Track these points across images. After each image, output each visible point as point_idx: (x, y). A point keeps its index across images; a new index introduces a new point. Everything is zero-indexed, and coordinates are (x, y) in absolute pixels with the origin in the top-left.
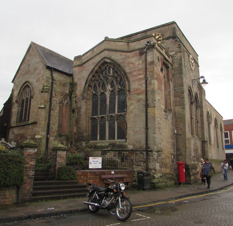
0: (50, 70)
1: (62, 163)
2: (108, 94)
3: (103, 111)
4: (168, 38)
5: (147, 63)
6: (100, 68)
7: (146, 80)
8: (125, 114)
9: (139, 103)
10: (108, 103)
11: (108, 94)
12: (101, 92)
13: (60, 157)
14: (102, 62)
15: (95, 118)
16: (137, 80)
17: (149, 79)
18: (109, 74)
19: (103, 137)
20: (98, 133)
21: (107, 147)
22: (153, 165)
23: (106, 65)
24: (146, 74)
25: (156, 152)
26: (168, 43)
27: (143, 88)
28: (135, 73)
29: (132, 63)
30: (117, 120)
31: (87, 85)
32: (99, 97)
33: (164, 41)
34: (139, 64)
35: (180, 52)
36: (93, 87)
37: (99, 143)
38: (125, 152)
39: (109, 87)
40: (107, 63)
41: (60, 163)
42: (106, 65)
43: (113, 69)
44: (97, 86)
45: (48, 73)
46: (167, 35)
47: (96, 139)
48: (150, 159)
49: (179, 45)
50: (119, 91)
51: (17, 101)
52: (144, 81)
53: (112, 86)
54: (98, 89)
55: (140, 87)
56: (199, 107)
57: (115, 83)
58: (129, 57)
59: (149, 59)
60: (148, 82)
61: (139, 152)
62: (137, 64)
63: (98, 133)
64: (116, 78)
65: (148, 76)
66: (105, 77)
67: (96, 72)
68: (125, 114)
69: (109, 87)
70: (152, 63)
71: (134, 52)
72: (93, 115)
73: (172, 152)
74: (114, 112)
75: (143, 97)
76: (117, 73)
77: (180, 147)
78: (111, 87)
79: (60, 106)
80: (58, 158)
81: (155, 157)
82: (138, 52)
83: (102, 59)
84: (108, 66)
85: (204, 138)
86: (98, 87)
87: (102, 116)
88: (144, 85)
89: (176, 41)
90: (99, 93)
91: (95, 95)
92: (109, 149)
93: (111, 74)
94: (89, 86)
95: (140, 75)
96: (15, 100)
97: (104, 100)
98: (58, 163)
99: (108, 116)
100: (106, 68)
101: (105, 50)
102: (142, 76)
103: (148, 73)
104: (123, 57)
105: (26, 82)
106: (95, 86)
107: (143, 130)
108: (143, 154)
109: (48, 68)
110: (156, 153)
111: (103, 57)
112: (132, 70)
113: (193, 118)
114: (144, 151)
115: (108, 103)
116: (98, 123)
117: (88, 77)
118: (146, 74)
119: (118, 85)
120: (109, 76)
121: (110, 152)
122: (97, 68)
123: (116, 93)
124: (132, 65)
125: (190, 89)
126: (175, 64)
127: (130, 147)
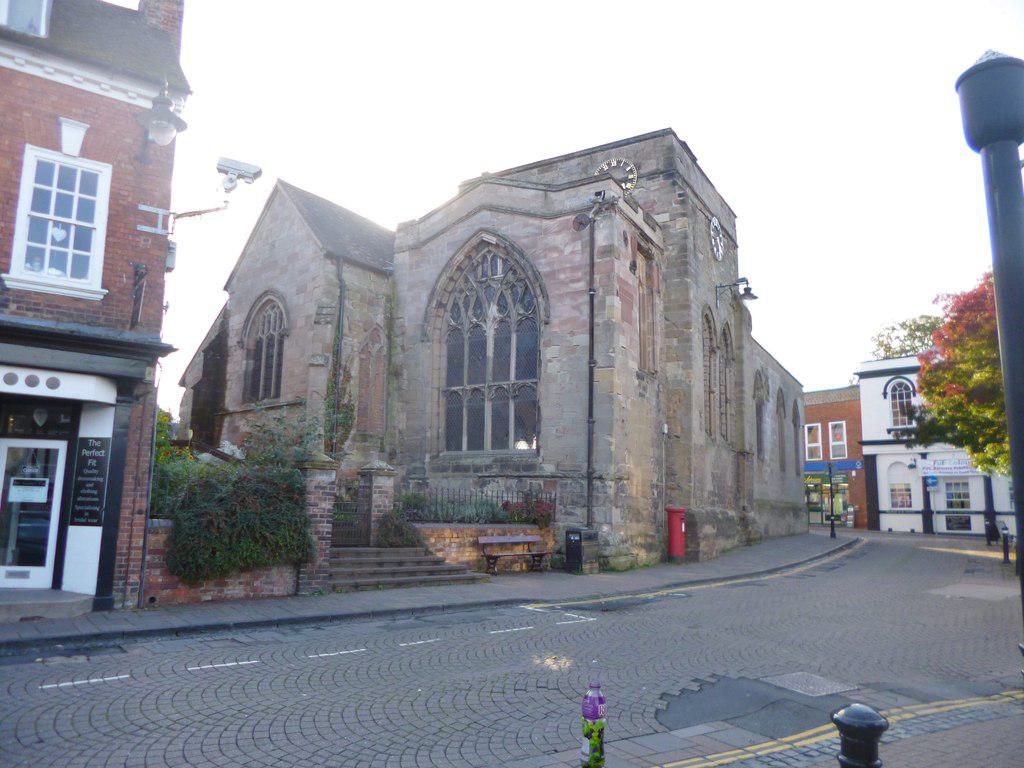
0: (334, 261)
1: (385, 507)
2: (490, 330)
3: (478, 375)
4: (651, 176)
5: (596, 251)
6: (468, 257)
7: (592, 297)
8: (536, 383)
9: (572, 356)
10: (490, 352)
11: (490, 330)
12: (471, 323)
13: (380, 492)
14: (475, 241)
15: (456, 392)
16: (568, 294)
17: (600, 292)
18: (493, 275)
19: (476, 443)
20: (465, 431)
21: (488, 467)
22: (605, 513)
23: (486, 249)
24: (591, 281)
25: (612, 480)
26: (652, 189)
27: (585, 316)
28: (562, 276)
29: (555, 249)
30: (514, 397)
31: (435, 302)
32: (466, 336)
33: (643, 182)
34: (573, 252)
35: (684, 215)
36: (449, 307)
37: (467, 457)
38: (534, 482)
39: (493, 311)
40: (489, 244)
41: (380, 506)
42: (486, 249)
43: (505, 261)
44: (461, 305)
45: (331, 268)
46: (651, 165)
47: (459, 448)
48: (597, 498)
49: (680, 195)
50: (520, 322)
51: (240, 343)
52: (586, 298)
53: (502, 307)
54: (463, 315)
55: (576, 314)
56: (733, 360)
57: (510, 300)
58: (546, 231)
59: (601, 240)
60: (596, 301)
61: (569, 481)
62: (568, 250)
63: (465, 431)
64: (513, 286)
65: (596, 285)
66: (481, 282)
67: (459, 269)
68: (536, 383)
69: (493, 311)
70: (609, 251)
71: (562, 219)
72: (450, 383)
73: (655, 481)
74: (507, 378)
75: (583, 339)
76: (515, 273)
77: (676, 468)
78: (500, 311)
79: (361, 360)
80: (374, 496)
81: (611, 492)
82: (572, 217)
83: (475, 234)
84: (489, 252)
85: (743, 445)
86: (463, 310)
87: (473, 386)
88: (586, 309)
89: (674, 184)
90: (467, 326)
91: (455, 331)
92: (495, 471)
93: (500, 274)
94: (440, 305)
95: (578, 280)
96: (236, 339)
97: (479, 345)
98: (376, 507)
99: (490, 387)
100: (484, 257)
101: (482, 208)
102: (582, 285)
103: (597, 277)
104: (530, 230)
105: (266, 293)
106: (455, 305)
107: (583, 427)
108: (582, 486)
109: (329, 256)
110: (612, 484)
111: (477, 228)
112: (556, 267)
113: (713, 392)
114: (583, 477)
115: (490, 352)
116: (465, 403)
117: (437, 282)
118: (591, 281)
119: (518, 306)
120: (494, 280)
121: (496, 480)
122: (460, 257)
123: (514, 327)
124: (555, 255)
125: (708, 312)
126: (671, 248)
127: (549, 469)
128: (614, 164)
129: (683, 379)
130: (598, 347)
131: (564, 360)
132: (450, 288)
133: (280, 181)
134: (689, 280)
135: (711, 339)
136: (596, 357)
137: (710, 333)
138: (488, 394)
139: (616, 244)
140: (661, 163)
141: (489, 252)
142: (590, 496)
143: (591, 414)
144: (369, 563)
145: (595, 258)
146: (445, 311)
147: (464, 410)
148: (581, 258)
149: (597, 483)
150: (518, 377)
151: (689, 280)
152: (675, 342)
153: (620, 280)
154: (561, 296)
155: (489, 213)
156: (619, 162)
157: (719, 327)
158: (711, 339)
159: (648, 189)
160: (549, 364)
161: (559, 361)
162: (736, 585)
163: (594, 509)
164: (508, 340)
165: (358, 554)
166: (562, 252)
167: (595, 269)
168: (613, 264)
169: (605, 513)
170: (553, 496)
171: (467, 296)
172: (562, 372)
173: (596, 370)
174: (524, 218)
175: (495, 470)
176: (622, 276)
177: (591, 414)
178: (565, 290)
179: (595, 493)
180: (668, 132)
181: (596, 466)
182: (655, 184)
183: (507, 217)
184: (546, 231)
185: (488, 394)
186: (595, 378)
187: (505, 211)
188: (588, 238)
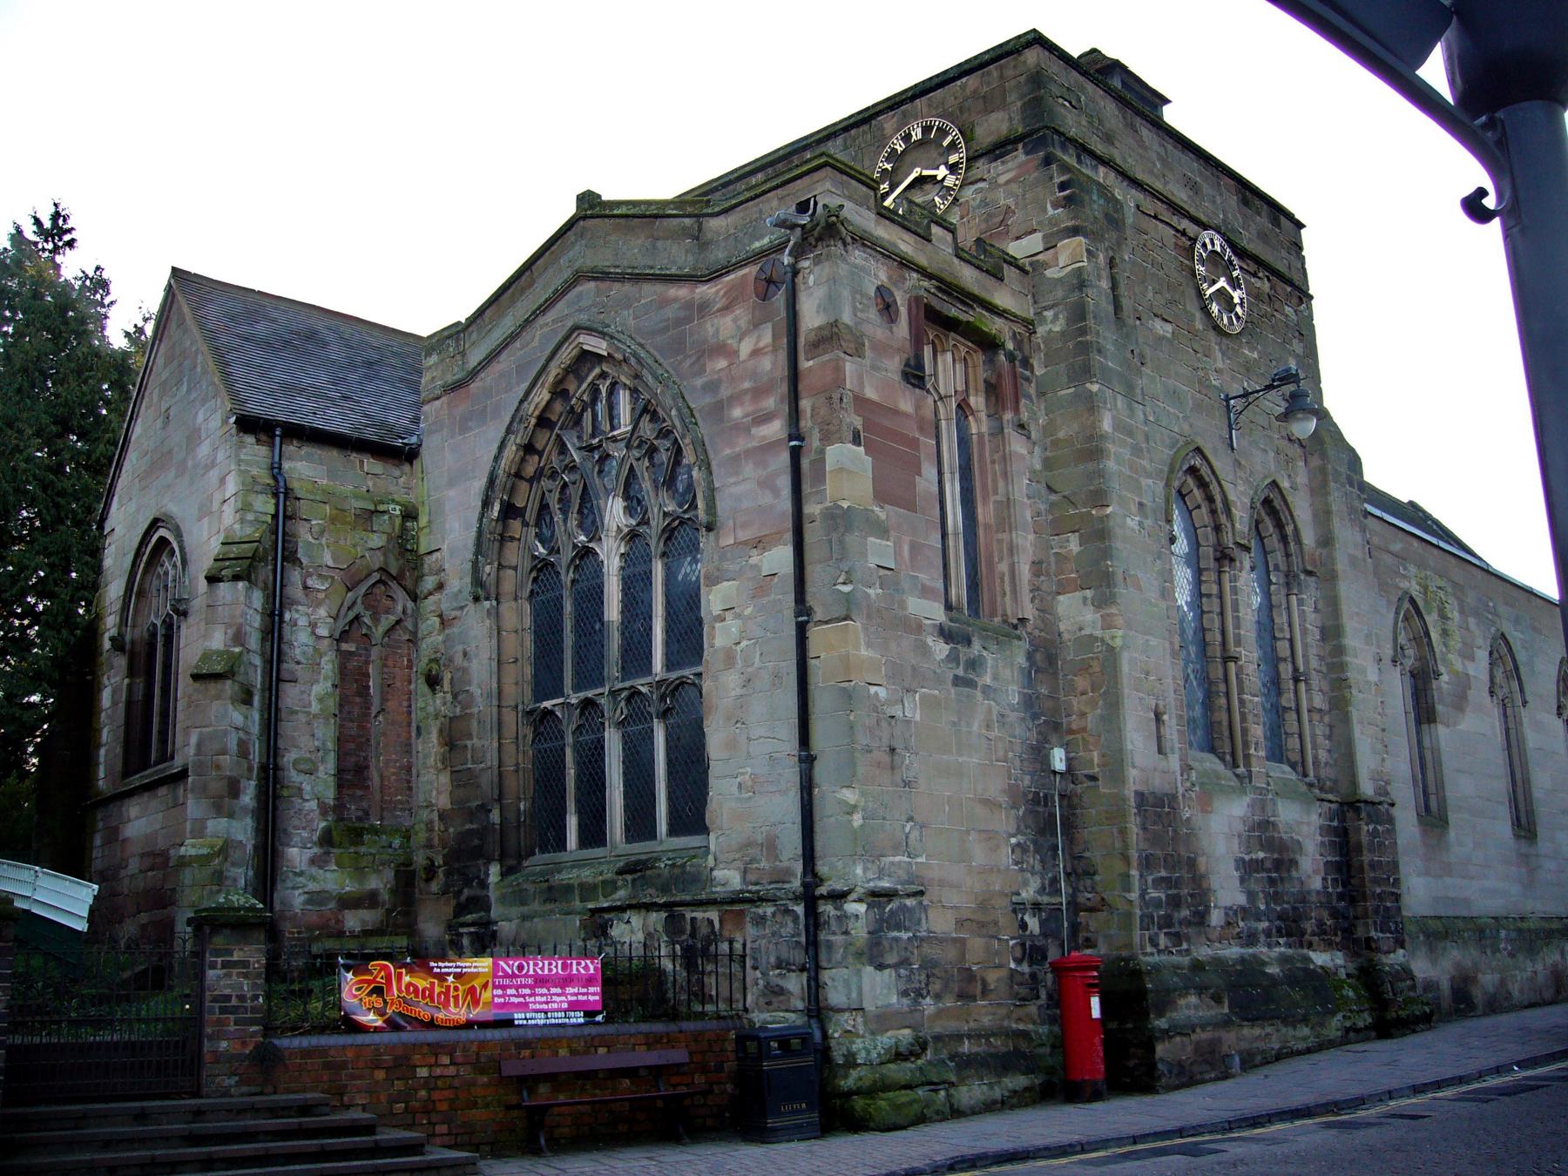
0: (263, 437)
1: (241, 998)
2: (611, 555)
3: (590, 673)
4: (999, 150)
5: (802, 341)
6: (559, 392)
7: (796, 454)
8: (699, 675)
9: (765, 600)
10: (613, 610)
11: (611, 555)
12: (575, 546)
13: (225, 965)
14: (566, 355)
15: (549, 713)
16: (748, 453)
17: (814, 441)
18: (613, 428)
19: (593, 833)
20: (571, 805)
21: (608, 886)
22: (847, 983)
23: (597, 371)
24: (795, 414)
25: (860, 900)
26: (1002, 179)
27: (786, 504)
28: (737, 413)
29: (721, 349)
30: (664, 715)
31: (497, 507)
32: (567, 577)
33: (981, 167)
34: (756, 353)
35: (1075, 231)
36: (531, 515)
37: (578, 864)
38: (699, 915)
39: (615, 513)
40: (599, 358)
41: (228, 998)
42: (597, 371)
43: (634, 391)
44: (555, 506)
45: (255, 452)
46: (995, 125)
47: (561, 844)
48: (830, 945)
49: (1063, 186)
50: (669, 534)
51: (118, 644)
52: (785, 458)
53: (633, 503)
54: (559, 529)
55: (766, 499)
56: (1310, 573)
57: (647, 485)
58: (703, 308)
59: (811, 318)
60: (805, 463)
61: (769, 910)
62: (745, 348)
63: (571, 805)
64: (652, 451)
65: (806, 423)
66: (591, 449)
67: (543, 422)
68: (699, 675)
69: (615, 513)
70: (829, 337)
71: (732, 276)
72: (540, 695)
73: (1028, 894)
74: (647, 668)
75: (780, 558)
76: (654, 417)
77: (1095, 855)
78: (629, 511)
79: (344, 657)
80: (211, 974)
81: (860, 931)
82: (751, 271)
83: (566, 338)
84: (603, 375)
86: (558, 517)
87: (582, 695)
88: (785, 483)
89: (1048, 161)
90: (567, 554)
91: (543, 568)
92: (621, 895)
93: (625, 427)
94: (509, 511)
95: (764, 419)
96: (113, 632)
97: (592, 598)
98: (215, 999)
99: (614, 694)
100: (595, 391)
101: (579, 277)
102: (776, 429)
103: (805, 404)
104: (670, 312)
105: (155, 524)
106: (544, 508)
107: (791, 775)
108: (796, 918)
109: (248, 424)
110: (861, 908)
111: (570, 324)
112: (725, 392)
113: (1236, 659)
114: (796, 899)
115: (613, 610)
116: (569, 739)
117: (497, 458)
118: (795, 414)
119: (664, 495)
120: (614, 440)
121: (626, 916)
122: (542, 396)
123: (656, 546)
124: (722, 363)
125: (1197, 462)
126: (1049, 314)
127: (729, 878)
128: (917, 134)
129: (1098, 633)
130: (816, 574)
131: (748, 611)
132: (530, 470)
133: (176, 272)
134: (1095, 388)
135: (1217, 528)
136: (811, 600)
137: (1213, 512)
138: (612, 711)
139: (846, 318)
140: (1017, 117)
141: (603, 375)
142: (813, 945)
143: (804, 739)
144: (166, 1139)
145: (801, 356)
146: (525, 524)
147: (569, 752)
148: (772, 365)
149: (827, 909)
150: (670, 665)
151: (1095, 388)
152: (1074, 544)
153: (861, 402)
154: (736, 459)
155: (592, 284)
156: (927, 130)
157: (1240, 497)
158: (1217, 528)
159: (994, 185)
160: (718, 625)
161: (738, 616)
162: (1091, 1162)
163: (825, 976)
164: (647, 578)
165: (141, 1117)
166: (736, 353)
167: (800, 387)
168: (838, 370)
169: (847, 983)
170: (738, 946)
171: (565, 485)
172: (744, 643)
173: (814, 633)
174: (659, 288)
175: (622, 893)
176: (870, 393)
177: (804, 739)
178: (742, 444)
179: (823, 936)
180: (1094, 51)
181: (822, 868)
182: (1005, 170)
183: (627, 288)
184: (703, 308)
185: (612, 711)
186: (813, 650)
187: (621, 278)
188: (783, 314)
